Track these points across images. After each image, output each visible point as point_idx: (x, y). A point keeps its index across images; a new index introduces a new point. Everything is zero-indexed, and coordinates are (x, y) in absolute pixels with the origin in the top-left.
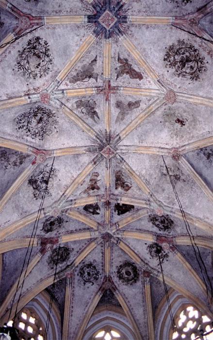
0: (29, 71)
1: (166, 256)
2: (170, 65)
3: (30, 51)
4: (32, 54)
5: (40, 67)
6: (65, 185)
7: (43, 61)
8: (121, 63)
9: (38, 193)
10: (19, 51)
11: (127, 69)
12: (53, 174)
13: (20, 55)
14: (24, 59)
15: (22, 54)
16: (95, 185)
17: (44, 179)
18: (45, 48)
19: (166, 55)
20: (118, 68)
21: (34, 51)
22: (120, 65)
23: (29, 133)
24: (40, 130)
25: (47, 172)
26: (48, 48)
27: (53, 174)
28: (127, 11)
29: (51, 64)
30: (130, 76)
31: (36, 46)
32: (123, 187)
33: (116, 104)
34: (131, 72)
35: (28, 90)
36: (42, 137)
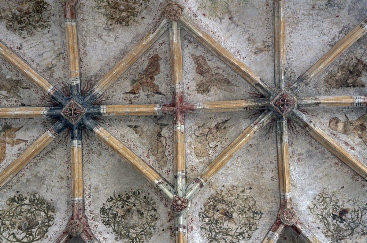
0: (146, 226)
1: (22, 33)
2: (134, 16)
3: (118, 222)
4: (123, 220)
5: (143, 210)
6: (353, 178)
7: (135, 206)
8: (138, 89)
9: (361, 226)
10: (116, 239)
11: (147, 80)
12: (331, 198)
13: (121, 239)
14: (129, 232)
15: (120, 235)
16: (358, 123)
17: (338, 215)
18: (117, 201)
19: (121, 23)
20: (147, 93)
21: (120, 217)
22: (141, 91)
23: (246, 235)
24: (244, 215)
25: (326, 208)
26: (117, 197)
27: (331, 198)
28: (65, 85)
29: (139, 193)
30: (156, 75)
31: (113, 214)
32: (359, 74)
33: (202, 93)
34: (150, 74)
35: (169, 230)
36: (256, 213)
